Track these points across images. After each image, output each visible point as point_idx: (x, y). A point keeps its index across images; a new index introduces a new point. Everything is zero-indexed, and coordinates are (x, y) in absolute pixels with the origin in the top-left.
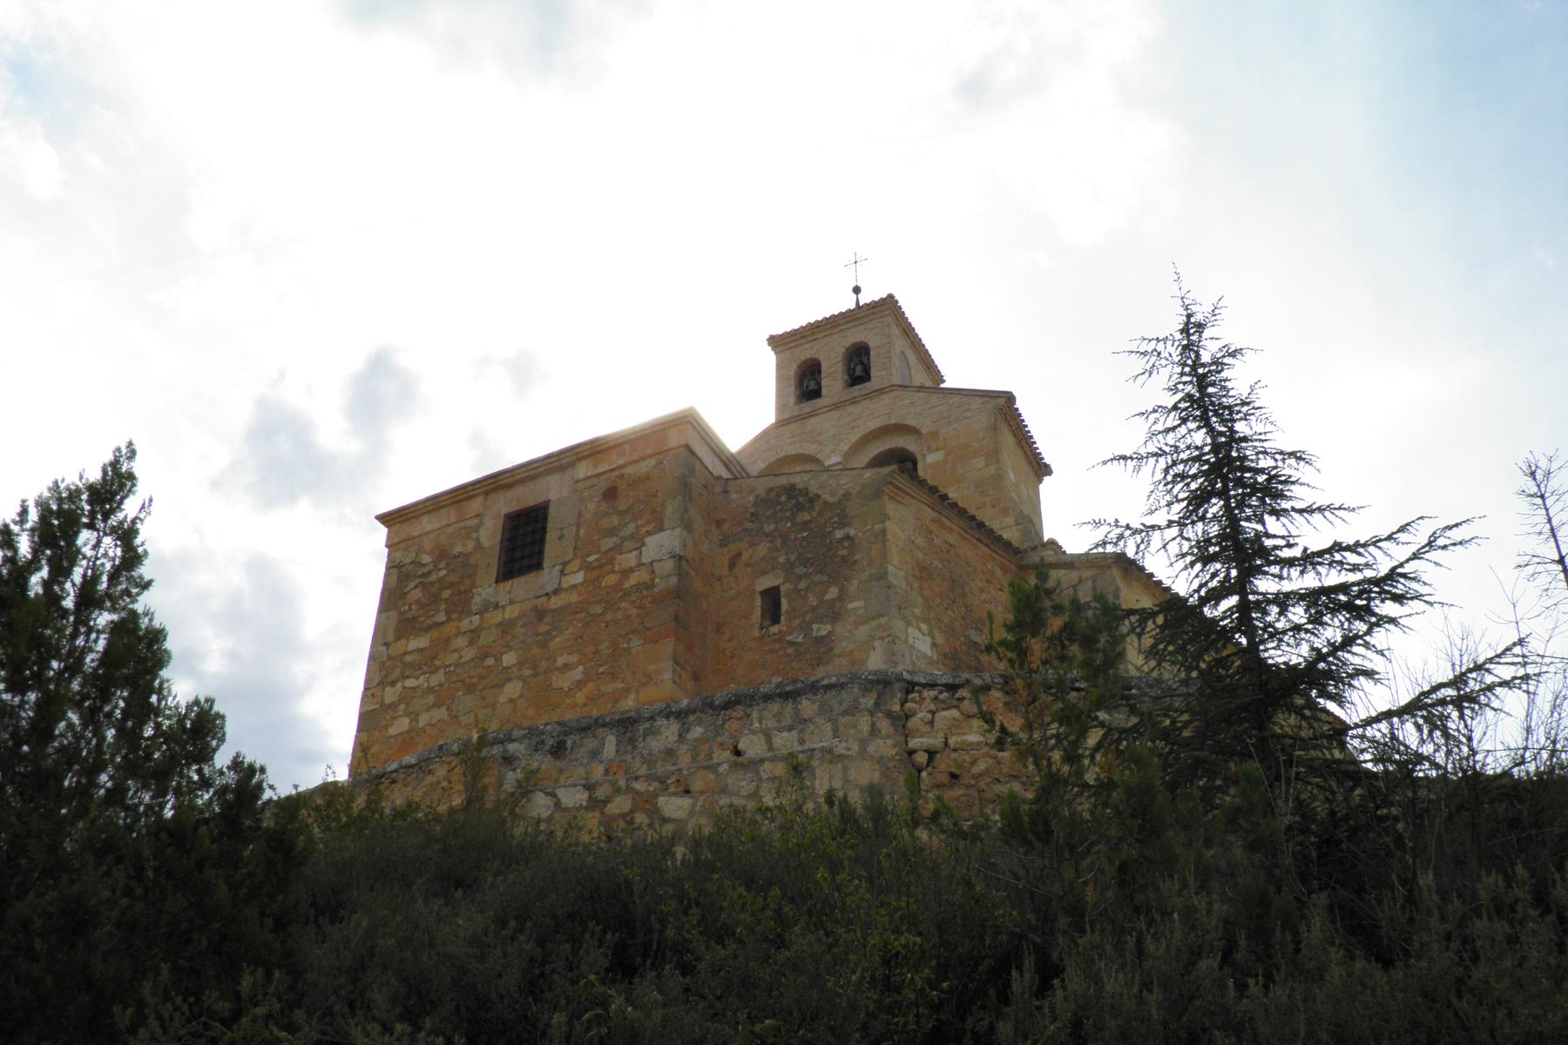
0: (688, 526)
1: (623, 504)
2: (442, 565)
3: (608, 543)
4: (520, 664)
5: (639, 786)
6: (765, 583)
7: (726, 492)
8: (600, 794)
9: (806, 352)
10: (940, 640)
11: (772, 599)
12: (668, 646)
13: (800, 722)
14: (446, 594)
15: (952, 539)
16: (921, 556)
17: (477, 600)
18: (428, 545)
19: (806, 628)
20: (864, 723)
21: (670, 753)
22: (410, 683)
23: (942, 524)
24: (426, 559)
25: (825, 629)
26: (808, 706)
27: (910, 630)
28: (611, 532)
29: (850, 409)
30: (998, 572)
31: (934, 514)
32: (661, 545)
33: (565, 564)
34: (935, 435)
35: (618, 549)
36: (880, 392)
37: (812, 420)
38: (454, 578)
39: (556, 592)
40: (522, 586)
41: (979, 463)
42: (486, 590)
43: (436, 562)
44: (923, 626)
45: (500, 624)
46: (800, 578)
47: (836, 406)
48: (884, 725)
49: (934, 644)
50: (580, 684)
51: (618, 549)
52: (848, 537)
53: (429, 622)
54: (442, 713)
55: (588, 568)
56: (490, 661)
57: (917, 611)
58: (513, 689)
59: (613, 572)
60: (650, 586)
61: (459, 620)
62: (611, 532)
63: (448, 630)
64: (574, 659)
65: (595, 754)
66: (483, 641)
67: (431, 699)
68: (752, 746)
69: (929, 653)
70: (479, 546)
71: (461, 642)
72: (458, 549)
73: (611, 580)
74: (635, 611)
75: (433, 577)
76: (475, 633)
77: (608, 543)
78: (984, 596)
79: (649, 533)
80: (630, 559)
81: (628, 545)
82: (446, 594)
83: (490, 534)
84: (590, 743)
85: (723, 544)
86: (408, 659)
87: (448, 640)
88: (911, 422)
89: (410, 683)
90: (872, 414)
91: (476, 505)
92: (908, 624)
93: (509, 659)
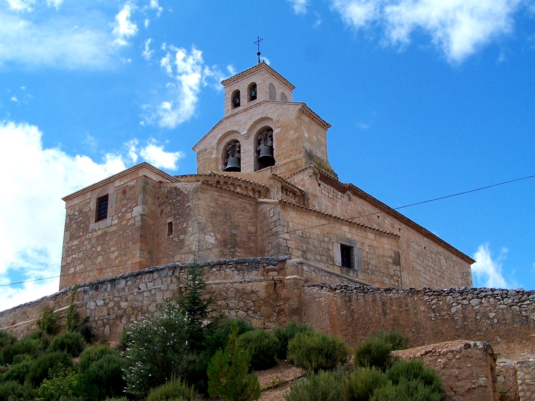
0: (145, 203)
1: (128, 195)
2: (81, 216)
3: (124, 209)
4: (102, 250)
5: (116, 299)
6: (169, 220)
7: (160, 187)
8: (106, 301)
9: (235, 88)
10: (219, 236)
11: (170, 224)
12: (139, 245)
13: (154, 280)
14: (82, 226)
15: (226, 200)
16: (212, 210)
17: (90, 228)
18: (77, 209)
19: (178, 236)
20: (169, 279)
21: (123, 289)
22: (74, 256)
23: (223, 196)
24: (77, 213)
25: (182, 237)
26: (156, 275)
27: (207, 237)
28: (125, 206)
29: (250, 111)
30: (248, 206)
31: (219, 194)
32: (138, 210)
33: (113, 216)
34: (278, 121)
35: (126, 212)
36: (260, 104)
37: (237, 116)
38: (84, 220)
39: (111, 226)
40: (102, 224)
41: (292, 132)
42: (93, 225)
43: (79, 214)
44: (212, 234)
45: (96, 237)
46: (177, 219)
47: (245, 110)
48: (175, 280)
49: (216, 239)
50: (117, 258)
51: (126, 212)
52: (189, 206)
53: (78, 235)
54: (82, 266)
55: (118, 218)
56: (94, 249)
57: (210, 229)
58: (100, 259)
59: (125, 220)
60: (134, 225)
61: (86, 235)
62: (125, 206)
63: (83, 238)
64: (115, 249)
65: (106, 289)
66: (92, 243)
67: (79, 262)
68: (142, 286)
69: (214, 242)
70: (90, 210)
71: (86, 242)
72: (85, 210)
73: (124, 222)
74: (130, 233)
75: (78, 220)
76: (90, 239)
77: (124, 209)
78: (240, 217)
79: (134, 207)
80: (129, 215)
81: (129, 210)
82: (82, 226)
83: (93, 205)
84: (104, 287)
85: (159, 206)
86: (73, 248)
87: (83, 242)
88: (269, 116)
89: (74, 256)
90: (257, 113)
91: (89, 195)
92: (206, 234)
93: (99, 249)
